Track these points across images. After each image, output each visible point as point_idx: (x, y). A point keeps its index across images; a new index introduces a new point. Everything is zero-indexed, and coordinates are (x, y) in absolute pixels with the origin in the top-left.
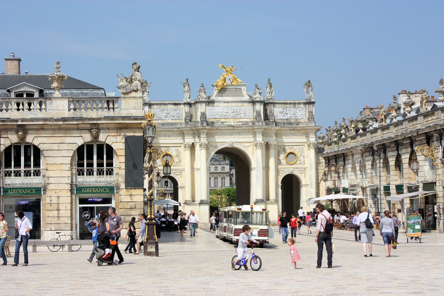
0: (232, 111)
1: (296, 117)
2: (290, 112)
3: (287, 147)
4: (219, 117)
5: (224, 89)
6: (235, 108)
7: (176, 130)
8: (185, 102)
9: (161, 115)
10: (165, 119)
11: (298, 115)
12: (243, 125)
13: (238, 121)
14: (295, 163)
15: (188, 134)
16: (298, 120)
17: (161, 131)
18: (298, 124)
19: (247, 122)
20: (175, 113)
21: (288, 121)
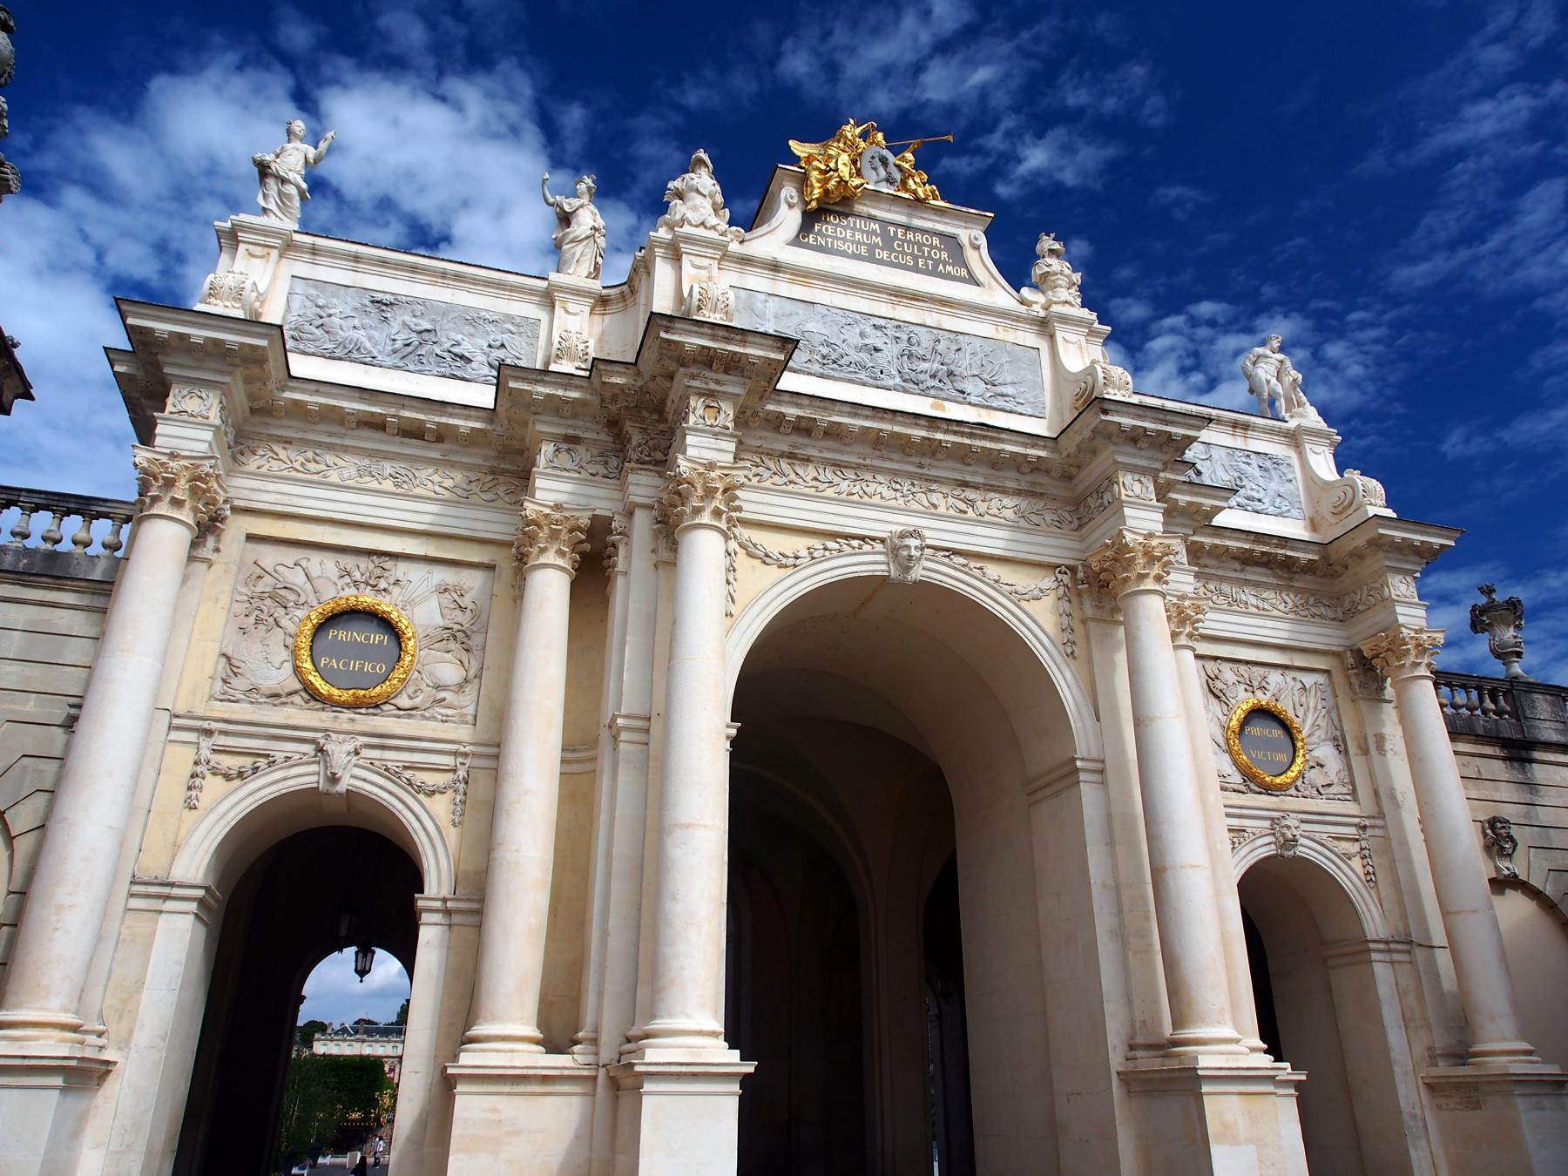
4: (816, 368)
10: (396, 360)
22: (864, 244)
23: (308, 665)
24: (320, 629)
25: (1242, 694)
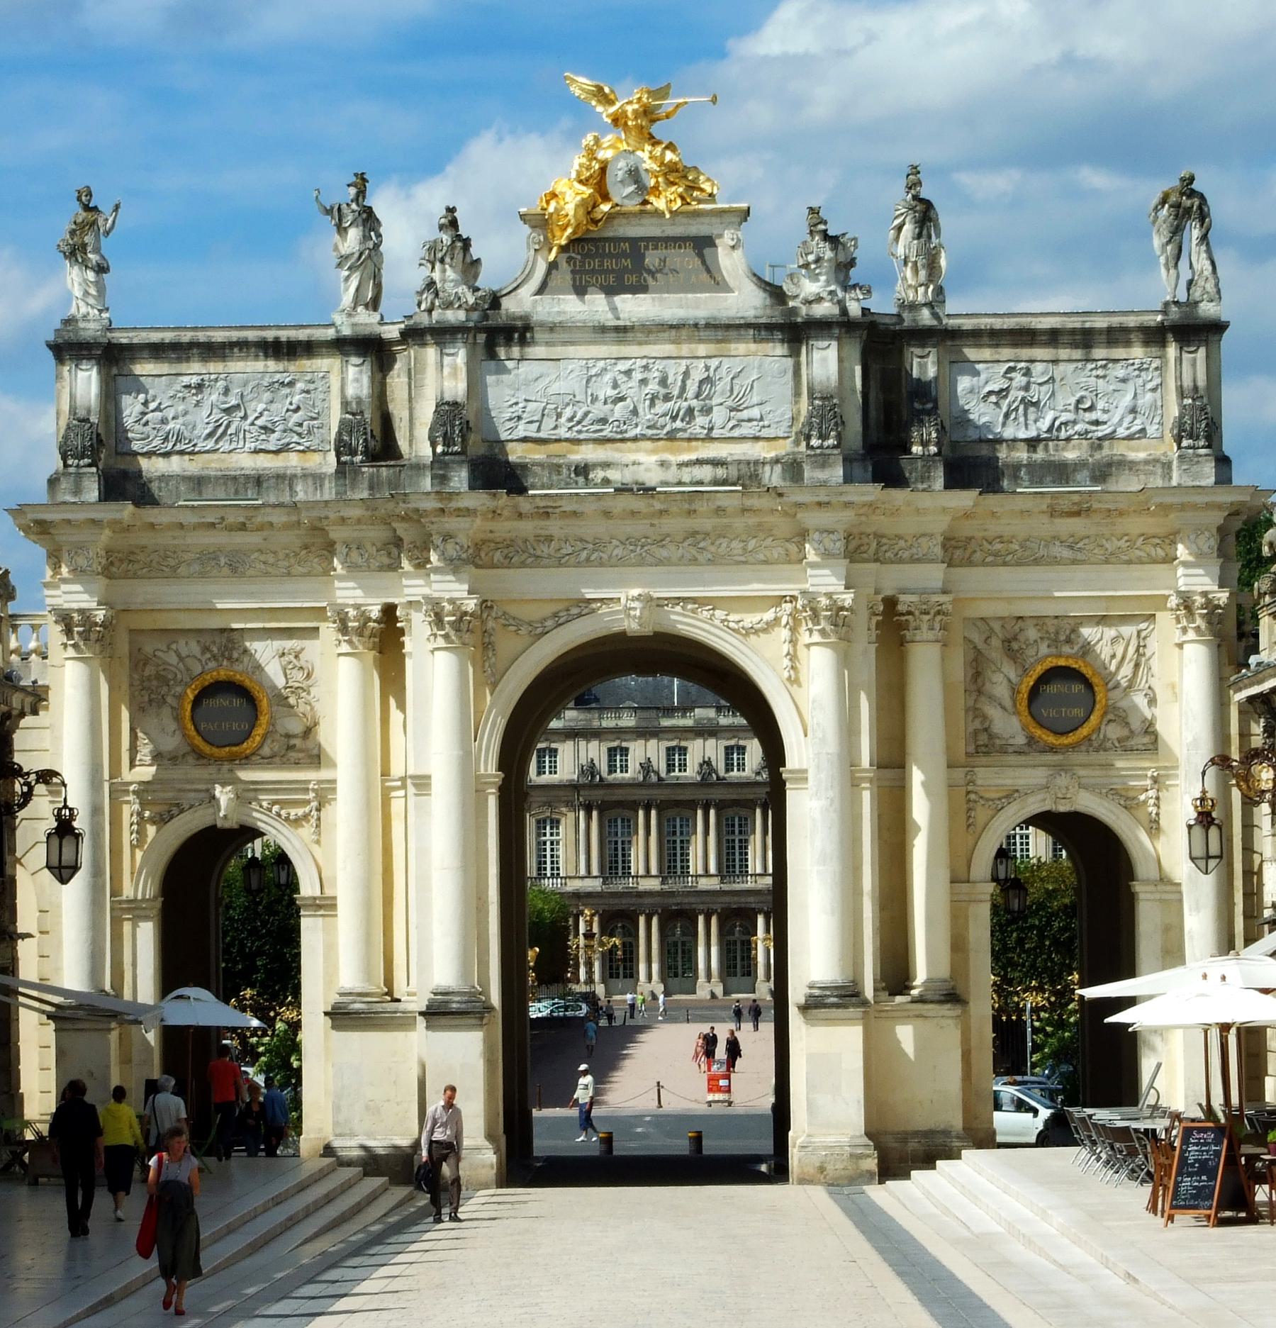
0: (653, 387)
1: (1097, 423)
2: (1053, 394)
3: (1032, 634)
4: (563, 433)
5: (592, 240)
6: (674, 371)
7: (278, 517)
8: (347, 332)
9: (181, 420)
10: (210, 444)
11: (1105, 411)
12: (724, 482)
13: (686, 457)
14: (1088, 738)
15: (354, 546)
16: (1111, 448)
17: (181, 526)
18: (1102, 473)
19: (748, 463)
20: (280, 408)
21: (1040, 455)
22: (613, 271)
23: (193, 733)
24: (197, 702)
25: (1044, 649)
